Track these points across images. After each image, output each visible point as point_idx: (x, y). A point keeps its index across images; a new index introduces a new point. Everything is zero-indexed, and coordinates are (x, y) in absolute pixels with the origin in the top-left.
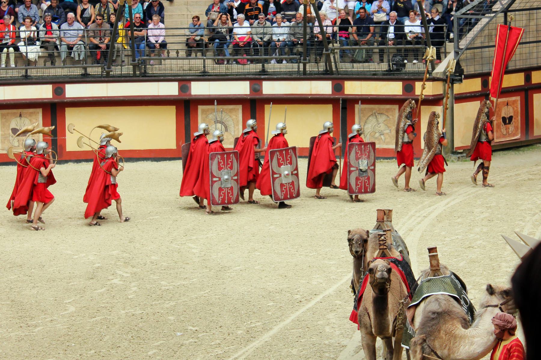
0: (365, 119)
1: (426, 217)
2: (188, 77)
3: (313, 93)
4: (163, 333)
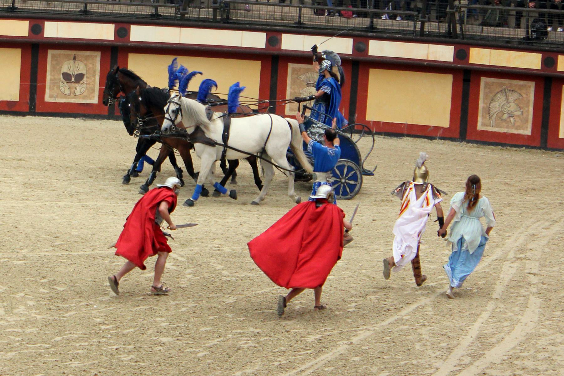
0: (491, 96)
1: (557, 222)
2: (278, 28)
3: (430, 59)
4: (218, 332)
